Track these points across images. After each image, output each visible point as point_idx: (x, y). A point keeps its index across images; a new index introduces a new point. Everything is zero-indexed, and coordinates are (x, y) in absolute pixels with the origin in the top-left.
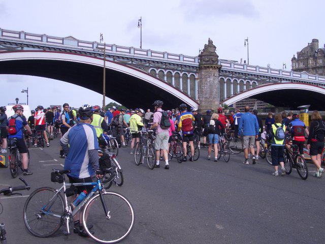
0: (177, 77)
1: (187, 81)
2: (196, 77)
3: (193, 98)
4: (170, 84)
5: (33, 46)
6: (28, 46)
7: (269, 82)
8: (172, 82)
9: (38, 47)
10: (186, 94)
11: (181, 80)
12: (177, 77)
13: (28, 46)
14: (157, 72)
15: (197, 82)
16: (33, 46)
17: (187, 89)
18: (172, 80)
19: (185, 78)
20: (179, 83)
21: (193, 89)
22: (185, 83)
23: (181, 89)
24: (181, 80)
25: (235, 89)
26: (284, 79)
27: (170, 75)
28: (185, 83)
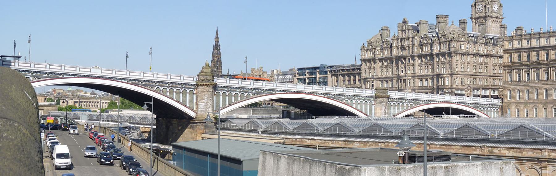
0: (178, 93)
1: (186, 96)
2: (195, 92)
3: (192, 109)
4: (172, 99)
5: (69, 75)
6: (66, 74)
7: (264, 93)
8: (173, 96)
9: (73, 75)
10: (185, 106)
11: (181, 94)
12: (178, 93)
13: (66, 74)
14: (161, 89)
15: (195, 96)
16: (69, 75)
17: (186, 102)
18: (173, 95)
19: (185, 93)
20: (180, 96)
21: (191, 101)
22: (184, 97)
23: (181, 101)
24: (181, 94)
25: (230, 100)
26: (278, 91)
27: (171, 91)
28: (184, 97)
